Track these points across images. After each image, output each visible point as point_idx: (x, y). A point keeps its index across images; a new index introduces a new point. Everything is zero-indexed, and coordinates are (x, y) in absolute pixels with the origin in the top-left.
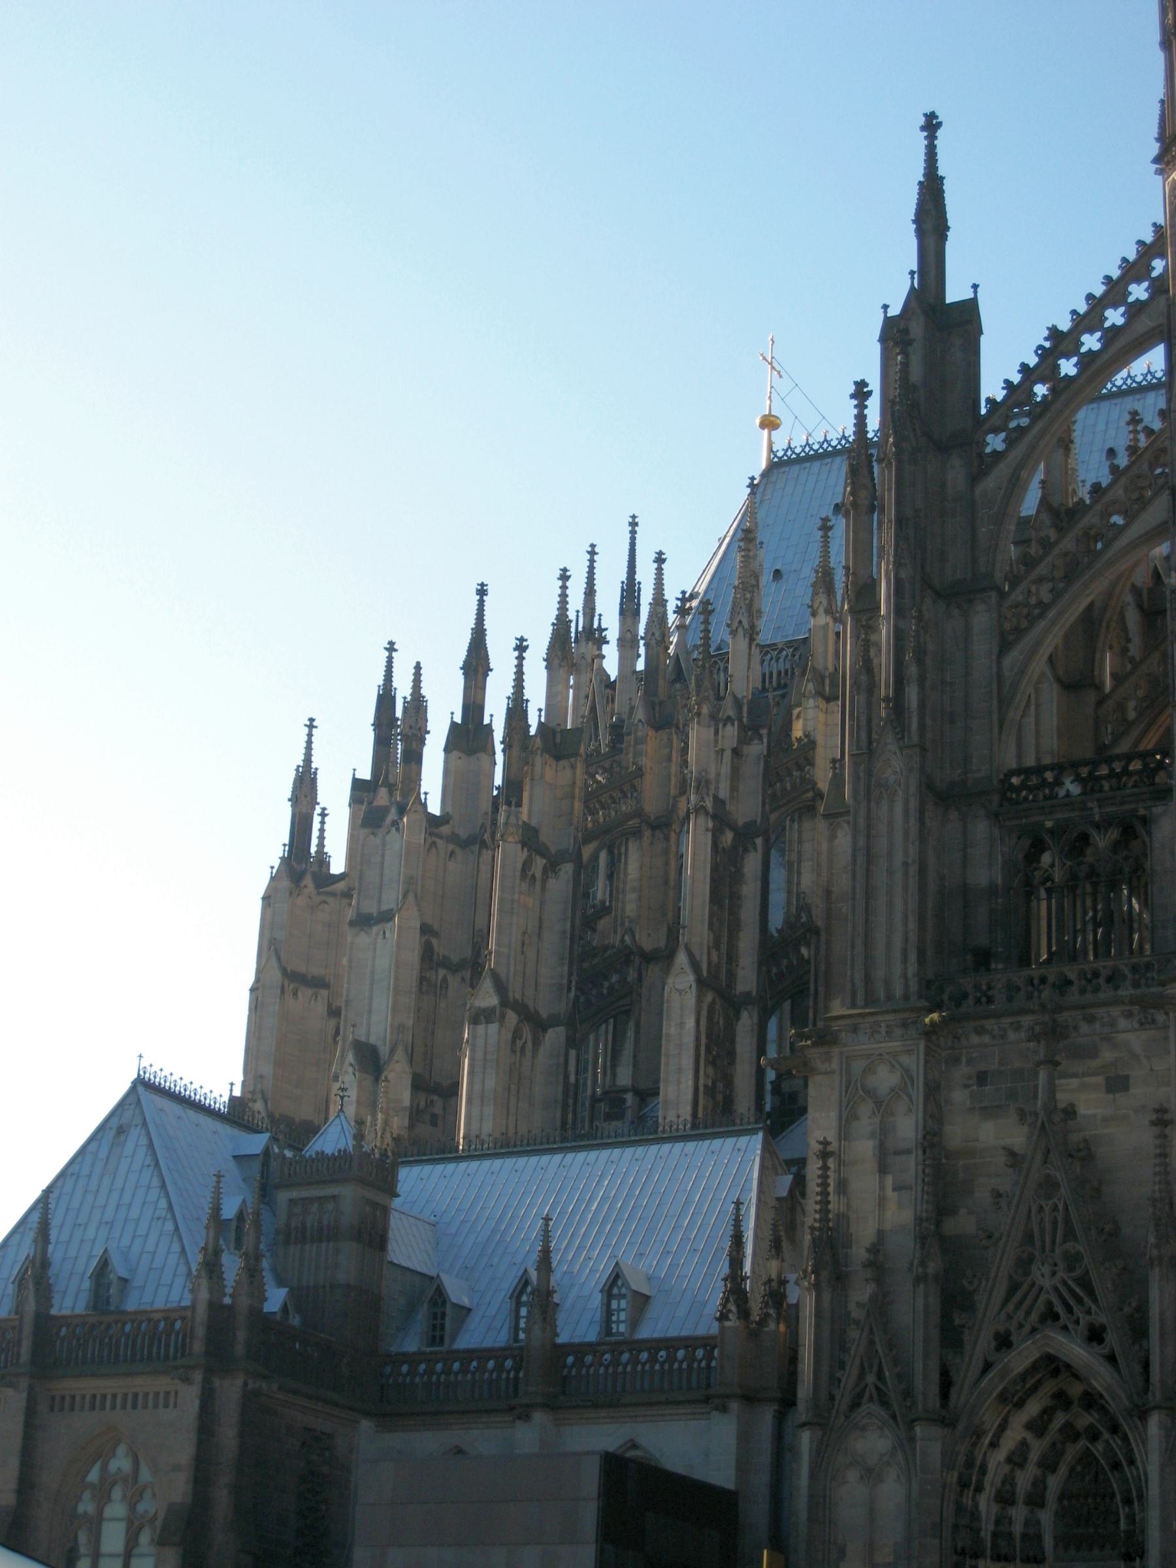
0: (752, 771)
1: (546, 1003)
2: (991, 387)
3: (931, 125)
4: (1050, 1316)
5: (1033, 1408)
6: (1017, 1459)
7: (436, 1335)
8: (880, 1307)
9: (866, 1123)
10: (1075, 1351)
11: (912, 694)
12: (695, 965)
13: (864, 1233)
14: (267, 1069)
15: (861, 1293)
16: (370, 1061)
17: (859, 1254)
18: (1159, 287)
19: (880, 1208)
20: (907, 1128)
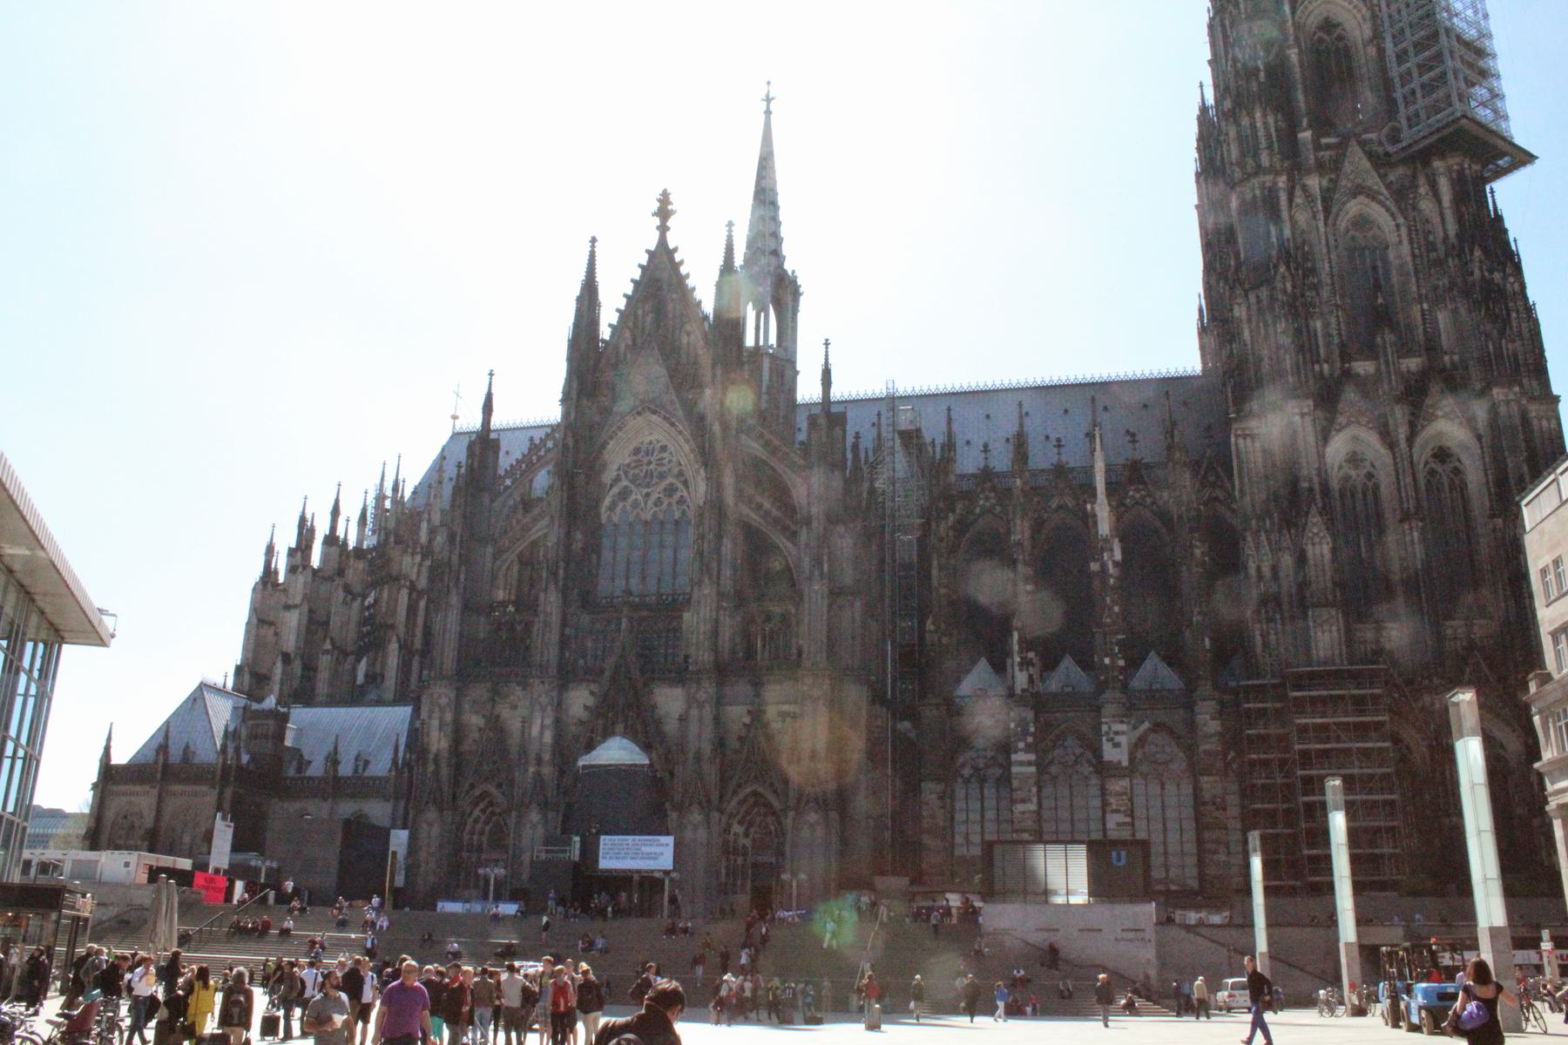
0: (425, 571)
1: (349, 649)
2: (501, 472)
3: (491, 374)
4: (487, 779)
5: (482, 806)
6: (476, 821)
7: (299, 770)
8: (436, 773)
9: (437, 714)
10: (493, 790)
11: (462, 576)
12: (399, 641)
13: (434, 749)
14: (250, 655)
15: (431, 768)
16: (286, 658)
17: (431, 756)
18: (555, 445)
19: (438, 741)
20: (449, 717)
